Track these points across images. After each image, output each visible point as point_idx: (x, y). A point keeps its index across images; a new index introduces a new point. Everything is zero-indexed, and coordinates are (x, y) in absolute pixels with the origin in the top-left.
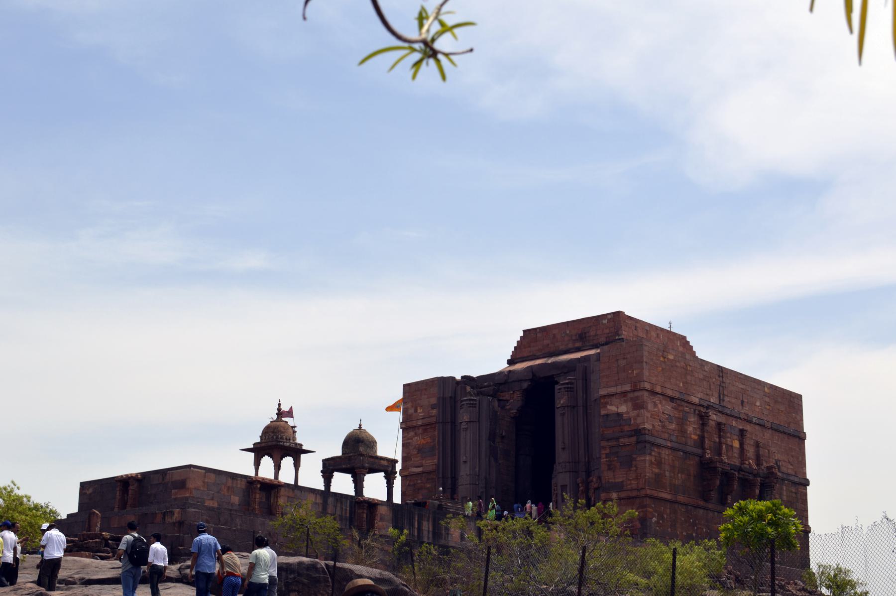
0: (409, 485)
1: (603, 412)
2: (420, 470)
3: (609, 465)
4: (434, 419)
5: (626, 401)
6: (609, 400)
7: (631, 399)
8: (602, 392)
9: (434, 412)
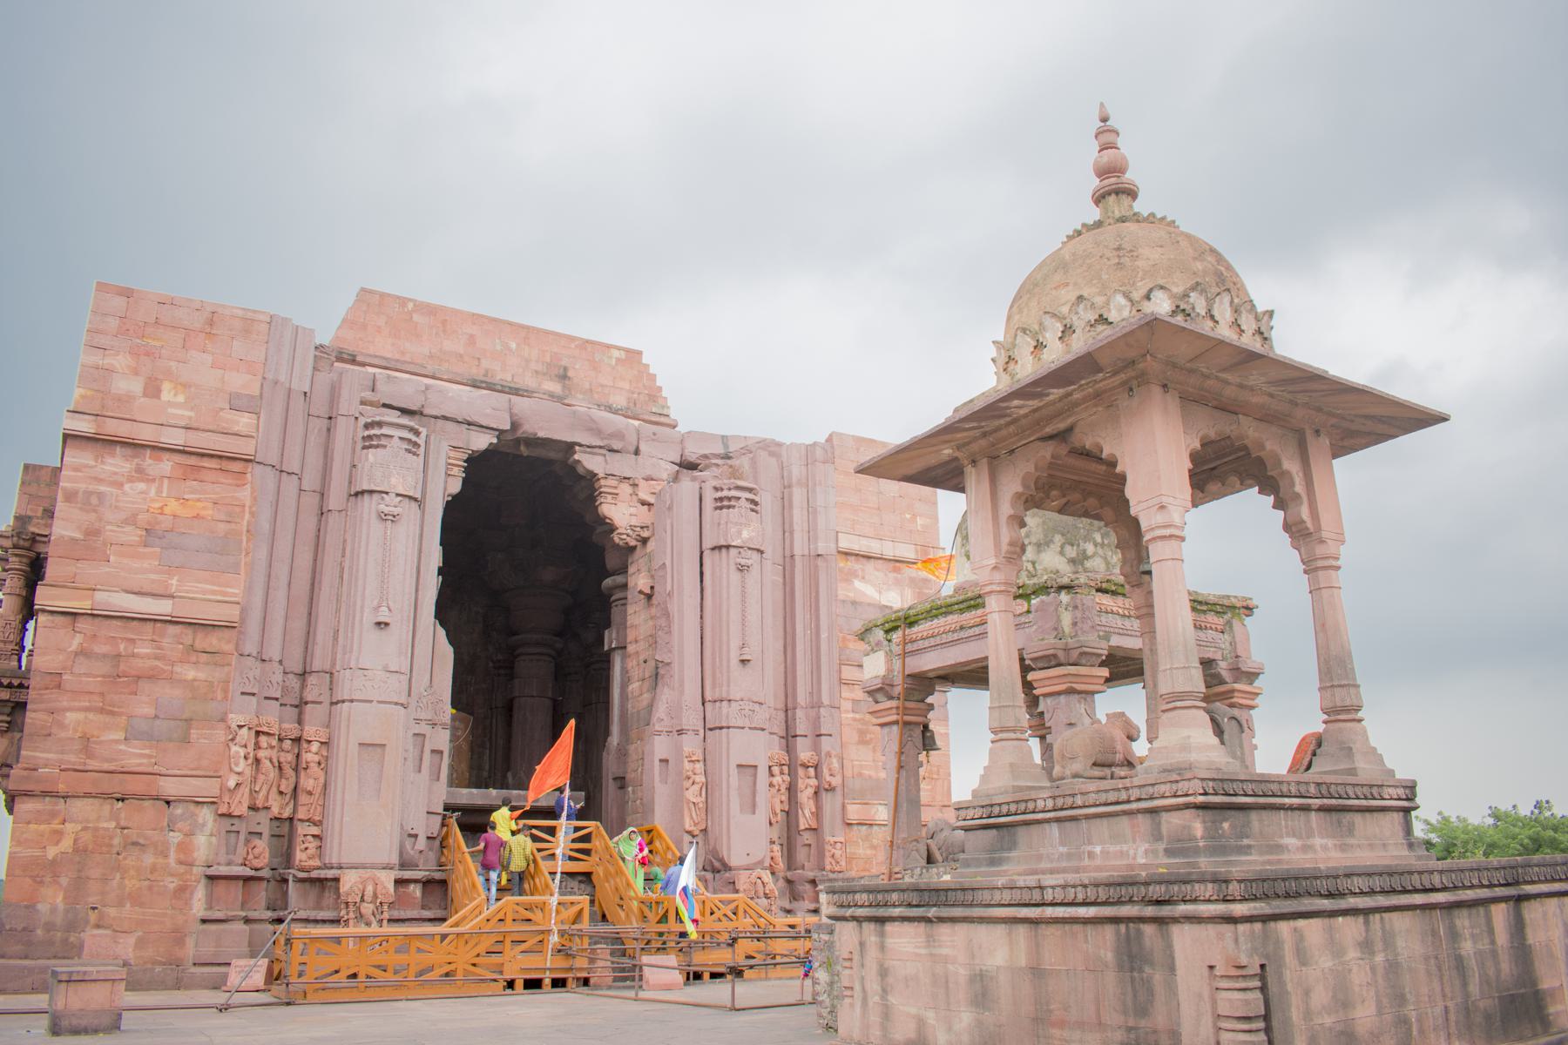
0: (82, 653)
1: (843, 592)
2: (162, 607)
3: (862, 733)
4: (246, 448)
5: (898, 582)
6: (857, 566)
7: (912, 580)
8: (844, 544)
9: (244, 422)
